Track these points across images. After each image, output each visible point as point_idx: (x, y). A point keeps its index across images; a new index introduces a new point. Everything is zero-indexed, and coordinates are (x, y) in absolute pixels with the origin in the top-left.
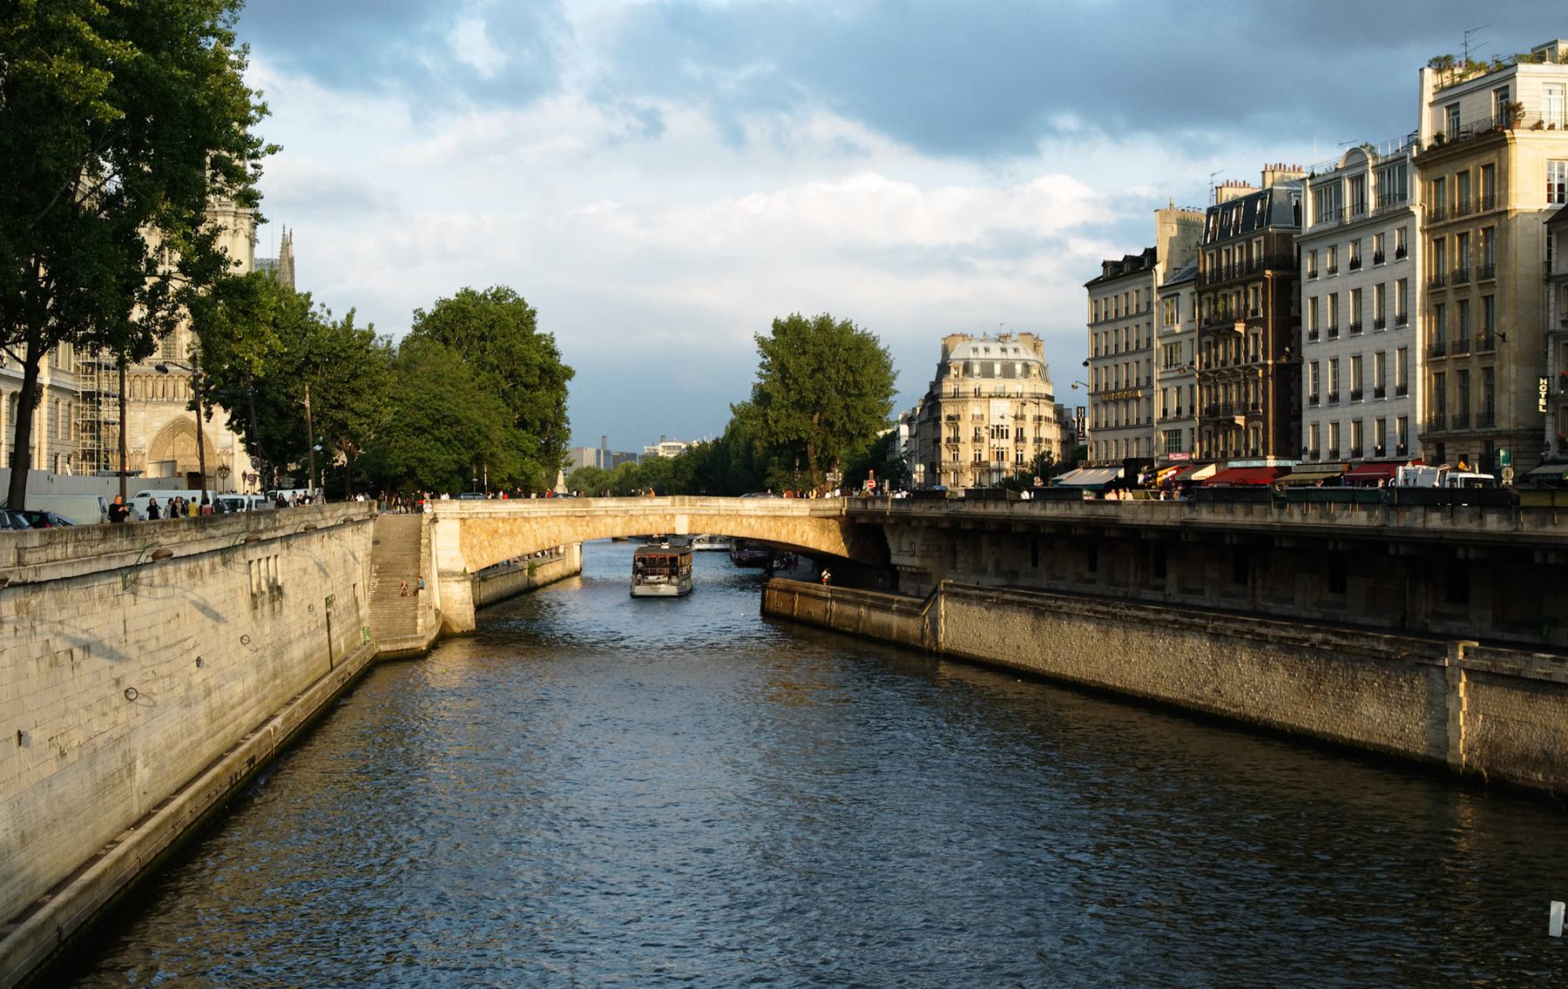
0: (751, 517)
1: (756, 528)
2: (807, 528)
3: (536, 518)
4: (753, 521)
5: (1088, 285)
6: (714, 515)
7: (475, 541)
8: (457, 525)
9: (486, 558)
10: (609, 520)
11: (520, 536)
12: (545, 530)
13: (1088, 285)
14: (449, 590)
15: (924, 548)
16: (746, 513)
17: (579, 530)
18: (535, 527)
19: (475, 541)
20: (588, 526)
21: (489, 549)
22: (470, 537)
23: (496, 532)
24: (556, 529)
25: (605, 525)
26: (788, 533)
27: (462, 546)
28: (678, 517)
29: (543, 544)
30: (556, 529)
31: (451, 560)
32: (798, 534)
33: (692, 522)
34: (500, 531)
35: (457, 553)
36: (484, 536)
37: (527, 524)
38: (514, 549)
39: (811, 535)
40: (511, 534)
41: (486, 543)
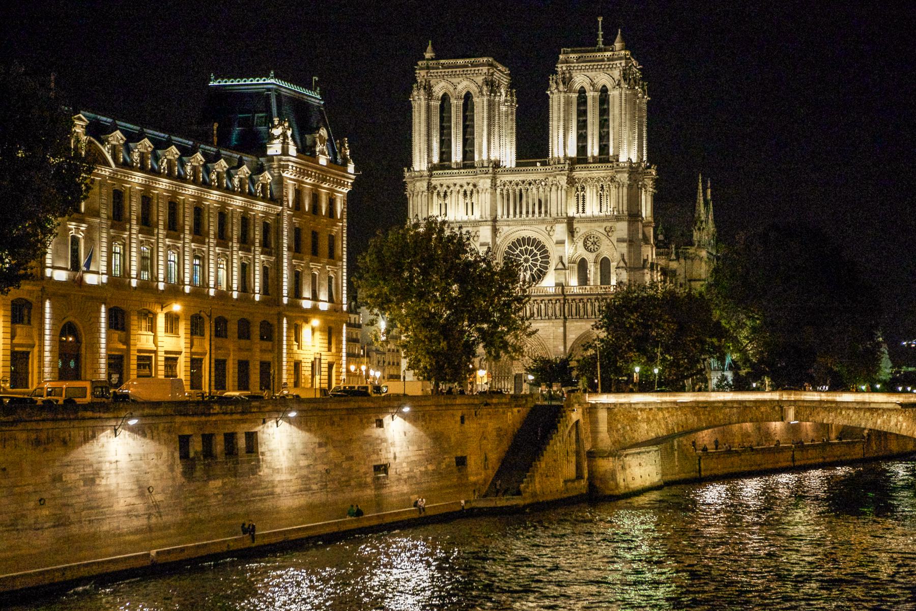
0: (849, 409)
1: (853, 418)
2: (901, 418)
7: (619, 426)
9: (628, 440)
12: (675, 417)
14: (594, 463)
17: (702, 417)
19: (619, 426)
20: (709, 415)
21: (630, 432)
22: (616, 423)
23: (636, 419)
26: (884, 422)
29: (673, 429)
32: (892, 423)
33: (797, 412)
34: (639, 418)
38: (650, 433)
39: (904, 424)
40: (648, 421)
41: (628, 428)
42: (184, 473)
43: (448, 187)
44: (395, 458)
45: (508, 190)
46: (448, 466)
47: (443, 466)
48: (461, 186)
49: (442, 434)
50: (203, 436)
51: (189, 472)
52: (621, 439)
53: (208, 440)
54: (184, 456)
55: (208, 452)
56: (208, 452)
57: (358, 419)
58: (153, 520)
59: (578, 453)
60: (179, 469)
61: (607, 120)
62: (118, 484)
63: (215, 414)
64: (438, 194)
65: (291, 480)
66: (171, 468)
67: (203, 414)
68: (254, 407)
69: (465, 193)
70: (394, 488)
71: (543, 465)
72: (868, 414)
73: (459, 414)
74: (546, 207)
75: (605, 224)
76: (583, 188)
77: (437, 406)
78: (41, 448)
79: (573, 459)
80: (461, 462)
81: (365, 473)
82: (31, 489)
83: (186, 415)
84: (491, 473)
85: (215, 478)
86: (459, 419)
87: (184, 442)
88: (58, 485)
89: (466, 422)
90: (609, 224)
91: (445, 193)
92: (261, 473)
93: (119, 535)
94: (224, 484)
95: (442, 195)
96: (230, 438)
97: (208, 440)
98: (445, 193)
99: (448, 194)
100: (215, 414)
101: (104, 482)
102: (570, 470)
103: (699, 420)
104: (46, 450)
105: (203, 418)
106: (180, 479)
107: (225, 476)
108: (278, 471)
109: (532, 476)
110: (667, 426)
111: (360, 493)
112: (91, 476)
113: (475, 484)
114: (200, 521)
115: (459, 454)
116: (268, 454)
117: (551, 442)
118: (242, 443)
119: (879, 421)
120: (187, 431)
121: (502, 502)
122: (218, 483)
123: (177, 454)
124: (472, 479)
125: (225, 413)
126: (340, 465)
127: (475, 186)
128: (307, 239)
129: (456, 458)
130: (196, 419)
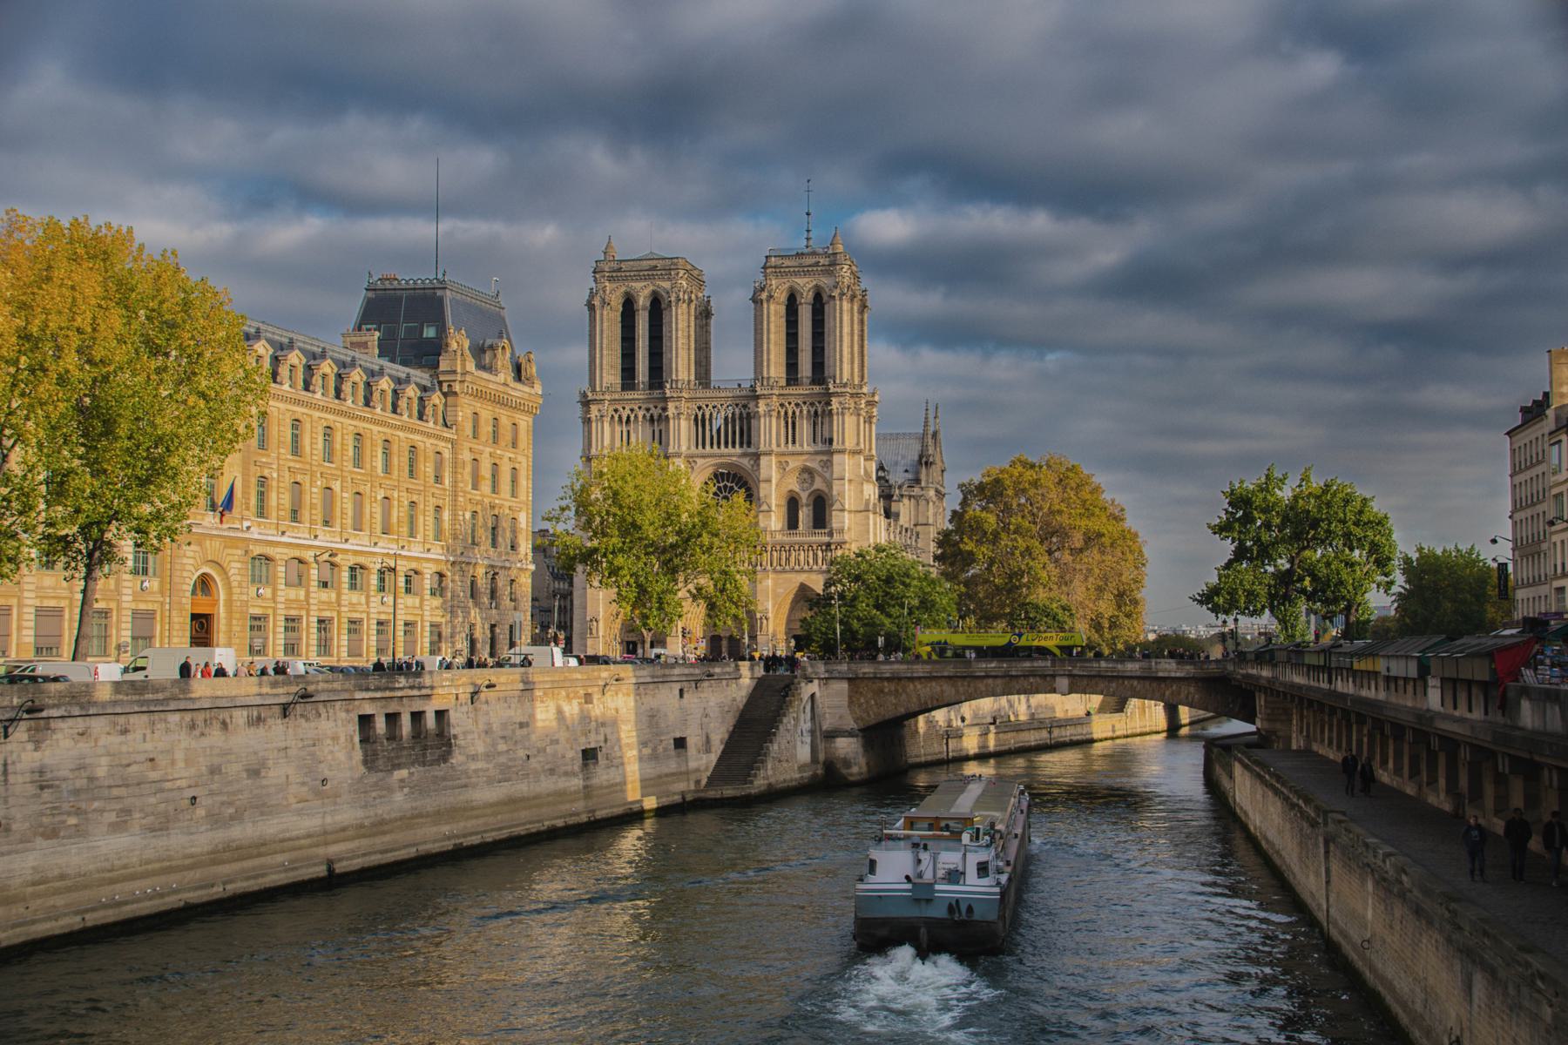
2: (1192, 689)
3: (920, 678)
4: (1135, 683)
5: (1508, 433)
6: (1094, 676)
8: (845, 685)
10: (990, 681)
11: (904, 696)
13: (1508, 433)
15: (1269, 711)
16: (1128, 674)
17: (961, 689)
18: (919, 687)
19: (862, 700)
23: (882, 691)
24: (938, 689)
25: (987, 685)
26: (1172, 693)
27: (851, 702)
28: (1058, 679)
30: (938, 689)
31: (841, 717)
35: (845, 711)
36: (870, 695)
37: (911, 686)
42: (365, 762)
43: (632, 410)
44: (606, 741)
45: (703, 415)
46: (665, 750)
47: (660, 749)
48: (648, 410)
49: (658, 711)
50: (388, 716)
51: (369, 762)
52: (865, 715)
53: (392, 718)
54: (365, 740)
55: (393, 735)
56: (393, 735)
57: (564, 693)
58: (329, 820)
59: (812, 732)
60: (358, 755)
61: (823, 333)
62: (287, 777)
63: (401, 689)
64: (620, 417)
65: (488, 770)
66: (350, 758)
67: (386, 689)
68: (447, 679)
69: (652, 419)
70: (605, 777)
71: (776, 747)
72: (1154, 685)
73: (677, 687)
74: (749, 436)
75: (819, 458)
76: (794, 413)
77: (653, 677)
78: (197, 733)
79: (808, 739)
80: (680, 743)
81: (573, 759)
82: (183, 783)
83: (368, 689)
84: (713, 758)
85: (398, 766)
86: (677, 692)
87: (365, 721)
88: (216, 777)
89: (685, 695)
90: (825, 458)
91: (628, 417)
92: (453, 761)
93: (290, 839)
94: (411, 774)
95: (625, 419)
96: (417, 717)
97: (392, 718)
98: (628, 417)
99: (632, 418)
100: (401, 689)
101: (271, 774)
102: (804, 753)
103: (957, 692)
104: (202, 734)
105: (388, 694)
106: (362, 769)
107: (413, 764)
108: (474, 758)
109: (763, 762)
110: (919, 700)
111: (567, 784)
112: (257, 767)
113: (697, 770)
114: (382, 822)
115: (678, 735)
116: (461, 737)
117: (785, 720)
118: (430, 722)
119: (1167, 693)
120: (368, 709)
121: (729, 792)
122: (404, 773)
123: (357, 739)
124: (693, 765)
125: (412, 688)
126: (545, 750)
127: (665, 409)
128: (486, 470)
129: (675, 739)
130: (378, 695)
